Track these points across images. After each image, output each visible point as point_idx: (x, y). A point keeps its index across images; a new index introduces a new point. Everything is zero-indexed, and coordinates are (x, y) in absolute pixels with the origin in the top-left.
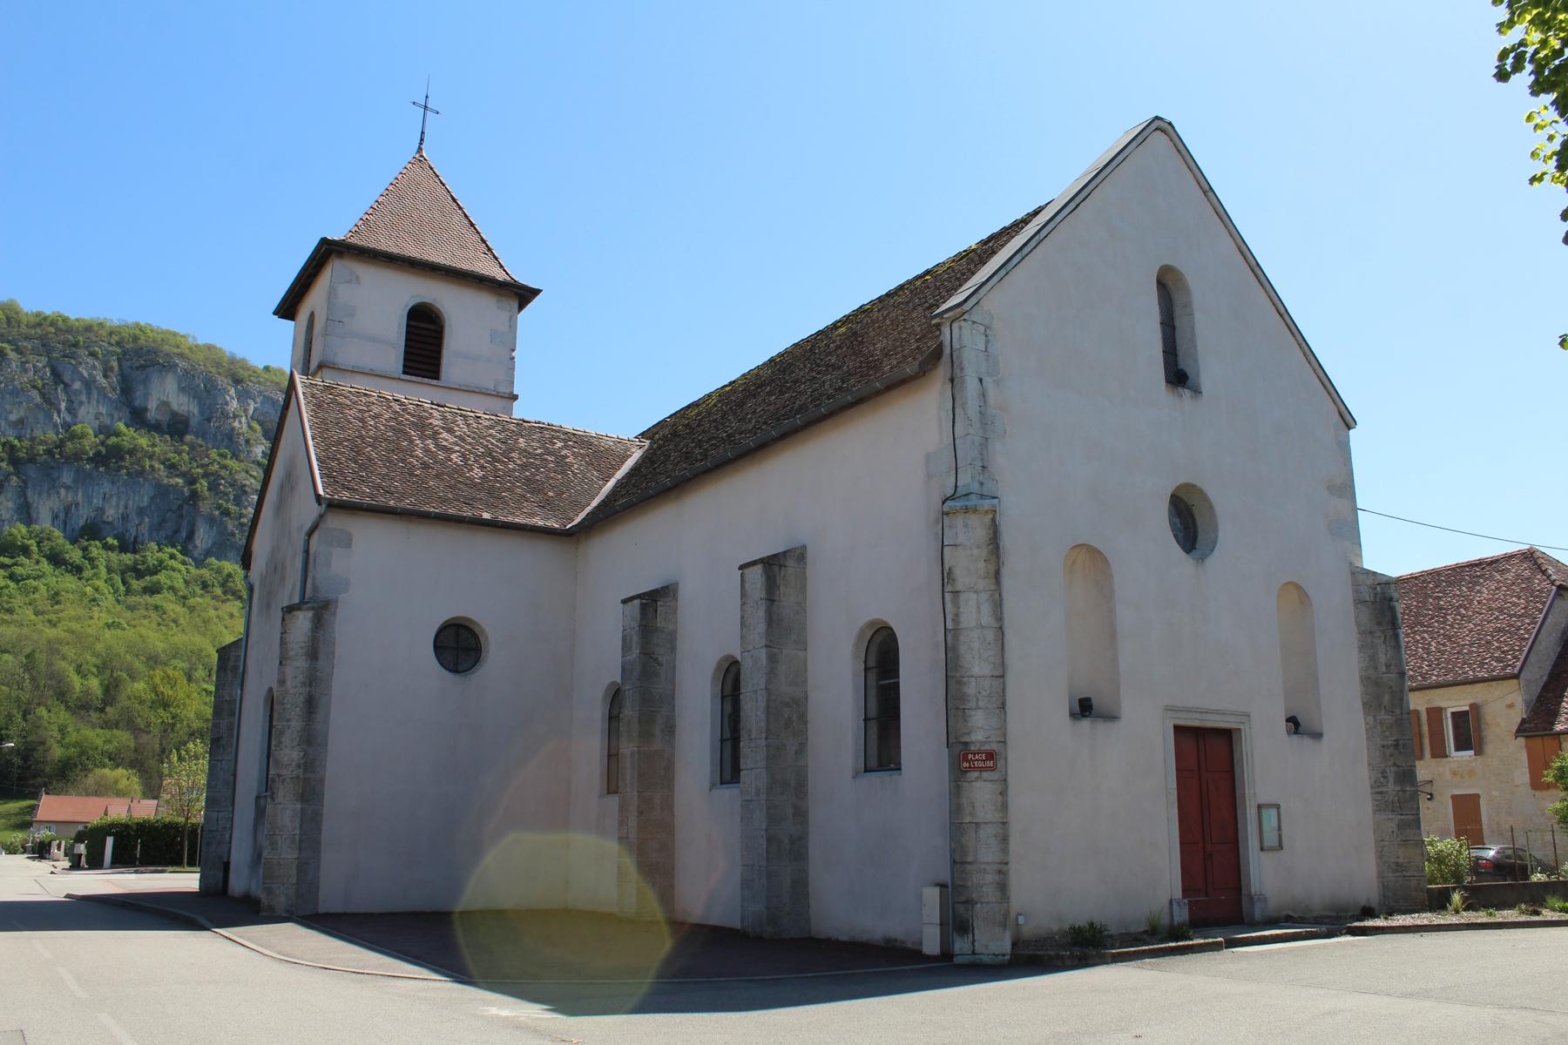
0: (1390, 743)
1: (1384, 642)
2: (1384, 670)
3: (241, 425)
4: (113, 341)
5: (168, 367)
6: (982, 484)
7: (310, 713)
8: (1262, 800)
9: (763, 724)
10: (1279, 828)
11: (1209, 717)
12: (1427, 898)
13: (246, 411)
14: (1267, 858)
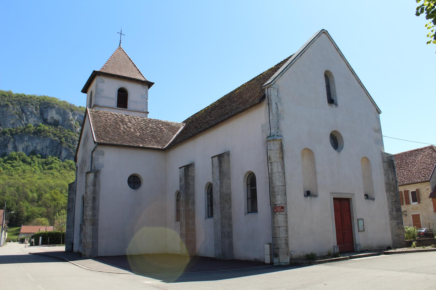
0: (394, 201)
1: (391, 173)
2: (391, 181)
3: (73, 123)
4: (38, 101)
5: (53, 107)
6: (278, 132)
7: (94, 201)
8: (359, 218)
9: (219, 201)
10: (364, 225)
11: (343, 195)
12: (405, 244)
13: (74, 119)
14: (360, 234)
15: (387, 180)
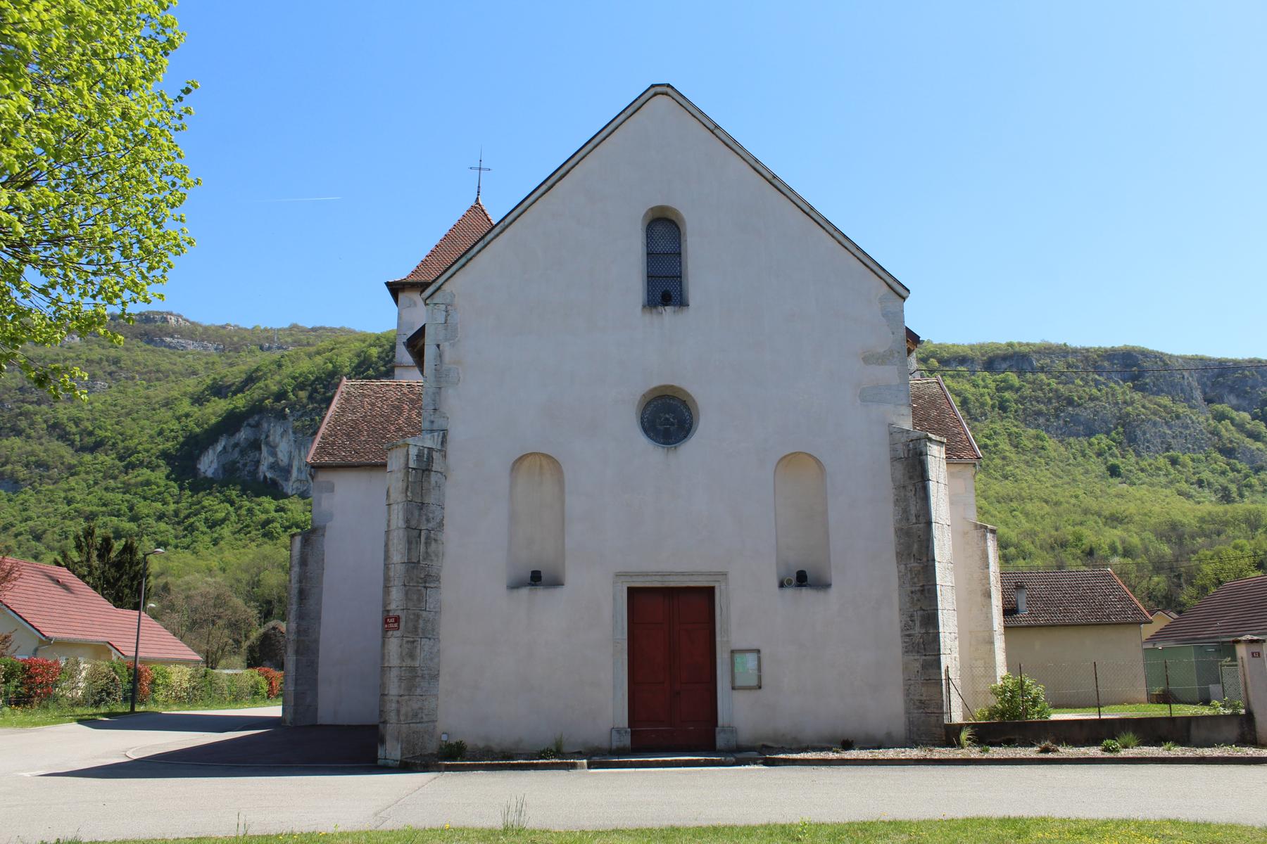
0: (917, 588)
1: (915, 495)
2: (914, 521)
6: (432, 422)
7: (302, 600)
11: (671, 578)
12: (944, 733)
15: (901, 520)
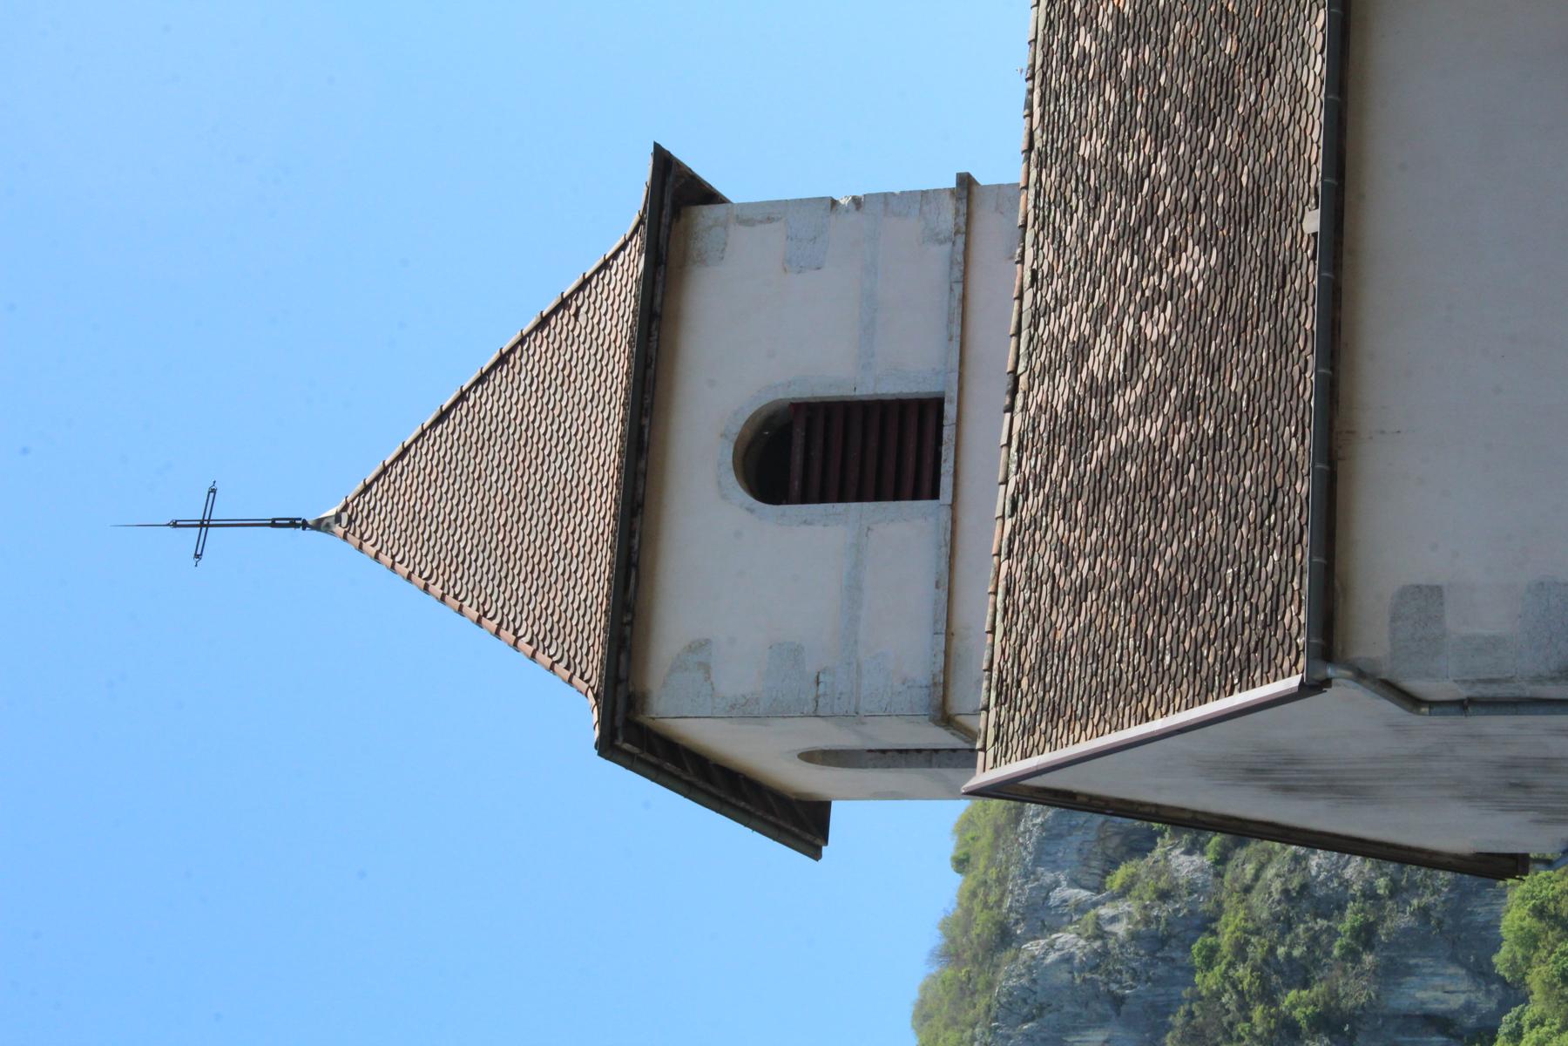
13: (1081, 908)
